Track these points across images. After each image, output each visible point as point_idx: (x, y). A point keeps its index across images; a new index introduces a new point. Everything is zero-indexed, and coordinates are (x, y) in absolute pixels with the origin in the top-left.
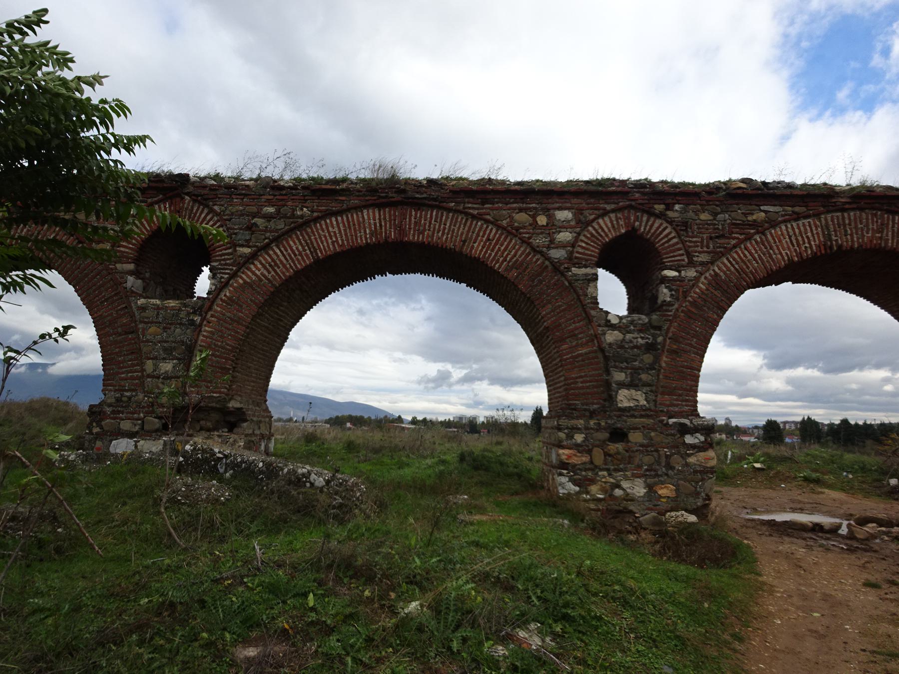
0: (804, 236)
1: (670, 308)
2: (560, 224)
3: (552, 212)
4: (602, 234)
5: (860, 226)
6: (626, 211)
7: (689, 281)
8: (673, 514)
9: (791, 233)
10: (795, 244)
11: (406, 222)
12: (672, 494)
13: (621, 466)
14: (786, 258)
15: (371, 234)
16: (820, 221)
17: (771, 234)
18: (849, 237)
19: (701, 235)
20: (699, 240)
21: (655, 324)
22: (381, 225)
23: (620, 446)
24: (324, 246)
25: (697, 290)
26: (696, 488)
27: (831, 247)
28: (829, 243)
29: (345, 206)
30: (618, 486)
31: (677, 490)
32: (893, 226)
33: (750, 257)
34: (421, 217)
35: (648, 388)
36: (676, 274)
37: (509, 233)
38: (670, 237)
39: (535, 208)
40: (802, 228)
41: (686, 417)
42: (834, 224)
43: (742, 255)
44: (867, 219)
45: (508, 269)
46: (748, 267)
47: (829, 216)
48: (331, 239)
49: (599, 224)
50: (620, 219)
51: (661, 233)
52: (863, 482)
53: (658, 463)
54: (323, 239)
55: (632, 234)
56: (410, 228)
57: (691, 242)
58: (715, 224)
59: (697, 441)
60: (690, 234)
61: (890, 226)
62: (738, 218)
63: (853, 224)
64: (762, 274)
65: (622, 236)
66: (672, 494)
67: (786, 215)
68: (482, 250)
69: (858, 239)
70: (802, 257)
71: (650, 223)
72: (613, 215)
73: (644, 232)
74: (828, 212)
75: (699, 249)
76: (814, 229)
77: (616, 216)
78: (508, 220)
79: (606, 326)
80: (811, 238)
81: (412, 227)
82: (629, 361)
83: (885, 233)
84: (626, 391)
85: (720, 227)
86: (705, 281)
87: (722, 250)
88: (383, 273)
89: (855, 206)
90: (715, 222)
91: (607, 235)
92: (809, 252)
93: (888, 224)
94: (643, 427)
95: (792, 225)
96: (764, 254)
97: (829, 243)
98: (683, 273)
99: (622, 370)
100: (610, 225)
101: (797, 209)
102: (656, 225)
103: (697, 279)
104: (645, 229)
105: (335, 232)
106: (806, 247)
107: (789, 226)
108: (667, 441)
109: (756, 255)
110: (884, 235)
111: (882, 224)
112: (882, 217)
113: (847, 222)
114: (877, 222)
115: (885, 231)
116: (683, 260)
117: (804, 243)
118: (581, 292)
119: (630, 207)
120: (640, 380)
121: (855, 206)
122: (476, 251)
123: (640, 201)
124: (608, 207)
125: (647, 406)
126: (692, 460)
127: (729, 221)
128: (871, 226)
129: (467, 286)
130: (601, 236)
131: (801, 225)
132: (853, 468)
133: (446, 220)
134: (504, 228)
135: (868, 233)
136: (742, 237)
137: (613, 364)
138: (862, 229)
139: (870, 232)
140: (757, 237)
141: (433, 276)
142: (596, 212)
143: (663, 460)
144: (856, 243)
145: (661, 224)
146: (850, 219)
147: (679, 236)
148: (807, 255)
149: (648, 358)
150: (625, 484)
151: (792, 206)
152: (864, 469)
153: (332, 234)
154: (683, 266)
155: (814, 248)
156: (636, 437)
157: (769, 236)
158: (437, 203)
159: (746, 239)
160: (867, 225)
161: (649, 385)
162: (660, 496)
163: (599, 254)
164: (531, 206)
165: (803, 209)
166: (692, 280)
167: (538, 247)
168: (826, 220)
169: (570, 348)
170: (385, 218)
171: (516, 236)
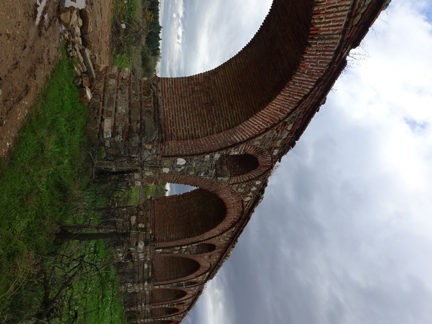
0: (331, 19)
5: (319, 61)
9: (340, 9)
10: (329, 10)
16: (337, 34)
18: (315, 52)
27: (312, 39)
28: (316, 38)
32: (308, 81)
40: (339, 19)
42: (330, 43)
44: (322, 66)
47: (338, 41)
52: (122, 9)
61: (309, 80)
67: (359, 7)
69: (310, 59)
70: (315, 14)
74: (342, 41)
76: (334, 28)
80: (327, 25)
83: (306, 76)
92: (316, 21)
93: (311, 78)
95: (346, 10)
97: (316, 38)
101: (359, 17)
106: (322, 19)
107: (347, 8)
110: (304, 75)
111: (313, 75)
113: (326, 53)
114: (316, 72)
115: (308, 76)
128: (315, 68)
132: (131, 4)
135: (311, 65)
138: (315, 62)
139: (311, 67)
144: (307, 57)
146: (328, 55)
148: (314, 19)
151: (363, 14)
152: (131, 10)
155: (318, 26)
160: (317, 66)
165: (356, 22)
168: (337, 38)
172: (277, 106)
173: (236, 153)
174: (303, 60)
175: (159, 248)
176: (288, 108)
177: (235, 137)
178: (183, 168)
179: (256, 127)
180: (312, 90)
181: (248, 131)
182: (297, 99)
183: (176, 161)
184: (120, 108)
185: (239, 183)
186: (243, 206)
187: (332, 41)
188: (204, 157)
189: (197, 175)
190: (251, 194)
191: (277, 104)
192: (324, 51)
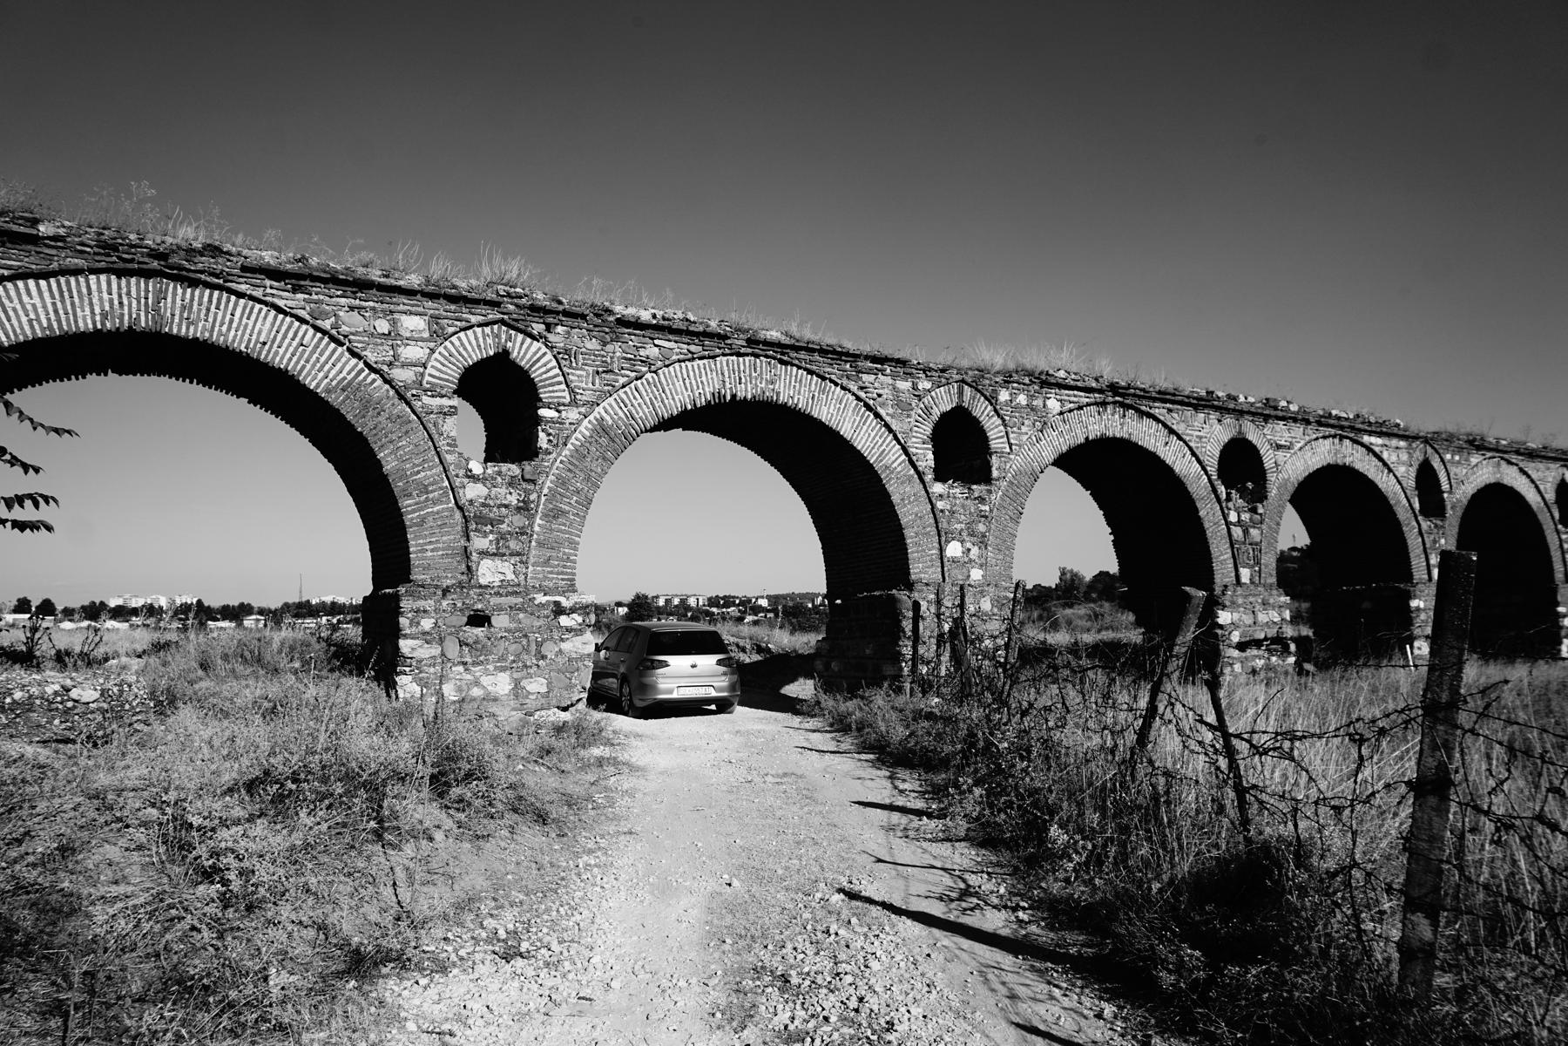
1: (549, 457)
2: (408, 335)
3: (396, 316)
4: (464, 353)
6: (496, 327)
7: (570, 424)
8: (543, 713)
9: (685, 376)
11: (165, 304)
12: (544, 689)
13: (482, 658)
14: (679, 405)
15: (104, 316)
17: (664, 374)
18: (743, 385)
19: (586, 368)
20: (584, 373)
21: (527, 477)
22: (121, 303)
23: (479, 632)
24: (12, 326)
25: (580, 437)
26: (570, 679)
27: (724, 396)
29: (55, 266)
30: (477, 683)
31: (549, 684)
33: (640, 400)
34: (192, 300)
35: (518, 559)
36: (556, 414)
37: (333, 339)
38: (549, 366)
39: (373, 309)
41: (563, 594)
42: (729, 370)
43: (632, 397)
44: (761, 367)
45: (328, 391)
46: (638, 414)
48: (27, 315)
49: (459, 339)
50: (488, 335)
51: (538, 360)
53: (526, 650)
54: (11, 313)
55: (503, 355)
56: (173, 315)
57: (573, 374)
58: (603, 356)
59: (574, 623)
60: (574, 365)
62: (628, 350)
63: (747, 371)
64: (651, 422)
65: (489, 359)
66: (544, 689)
68: (290, 359)
71: (525, 346)
72: (479, 330)
73: (517, 357)
75: (583, 385)
76: (709, 373)
77: (483, 331)
78: (333, 319)
79: (469, 477)
80: (706, 383)
81: (177, 312)
82: (494, 523)
84: (490, 562)
85: (609, 360)
86: (590, 426)
87: (610, 388)
88: (101, 370)
89: (749, 351)
90: (602, 353)
91: (470, 356)
94: (510, 607)
96: (656, 398)
98: (564, 414)
99: (485, 535)
100: (474, 342)
101: (693, 348)
102: (533, 349)
103: (579, 423)
104: (519, 353)
105: (34, 306)
108: (538, 624)
109: (647, 399)
112: (775, 367)
113: (742, 368)
116: (564, 398)
117: (698, 388)
118: (433, 431)
119: (503, 322)
120: (508, 547)
121: (749, 351)
122: (282, 358)
123: (515, 316)
124: (474, 319)
125: (516, 580)
126: (565, 646)
127: (618, 354)
129: (249, 402)
130: (463, 357)
131: (696, 367)
133: (234, 309)
134: (324, 332)
136: (633, 374)
137: (474, 526)
139: (764, 382)
140: (649, 376)
141: (191, 382)
142: (458, 323)
143: (533, 647)
145: (539, 349)
147: (560, 368)
149: (519, 520)
150: (485, 680)
151: (689, 344)
153: (29, 307)
154: (564, 405)
156: (500, 621)
157: (662, 376)
158: (221, 281)
159: (637, 379)
161: (518, 554)
162: (529, 693)
163: (460, 380)
164: (367, 304)
166: (573, 424)
167: (376, 363)
169: (417, 504)
170: (129, 293)
171: (342, 344)
172: (831, 411)
173: (931, 456)
174: (755, 397)
175: (1238, 577)
176: (833, 393)
177: (894, 466)
178: (969, 545)
179: (873, 434)
180: (799, 367)
181: (881, 445)
182: (816, 384)
183: (954, 560)
184: (868, 651)
185: (1007, 433)
186: (1080, 408)
187: (726, 368)
188: (942, 511)
189: (986, 517)
190: (1038, 403)
191: (828, 413)
192: (739, 372)
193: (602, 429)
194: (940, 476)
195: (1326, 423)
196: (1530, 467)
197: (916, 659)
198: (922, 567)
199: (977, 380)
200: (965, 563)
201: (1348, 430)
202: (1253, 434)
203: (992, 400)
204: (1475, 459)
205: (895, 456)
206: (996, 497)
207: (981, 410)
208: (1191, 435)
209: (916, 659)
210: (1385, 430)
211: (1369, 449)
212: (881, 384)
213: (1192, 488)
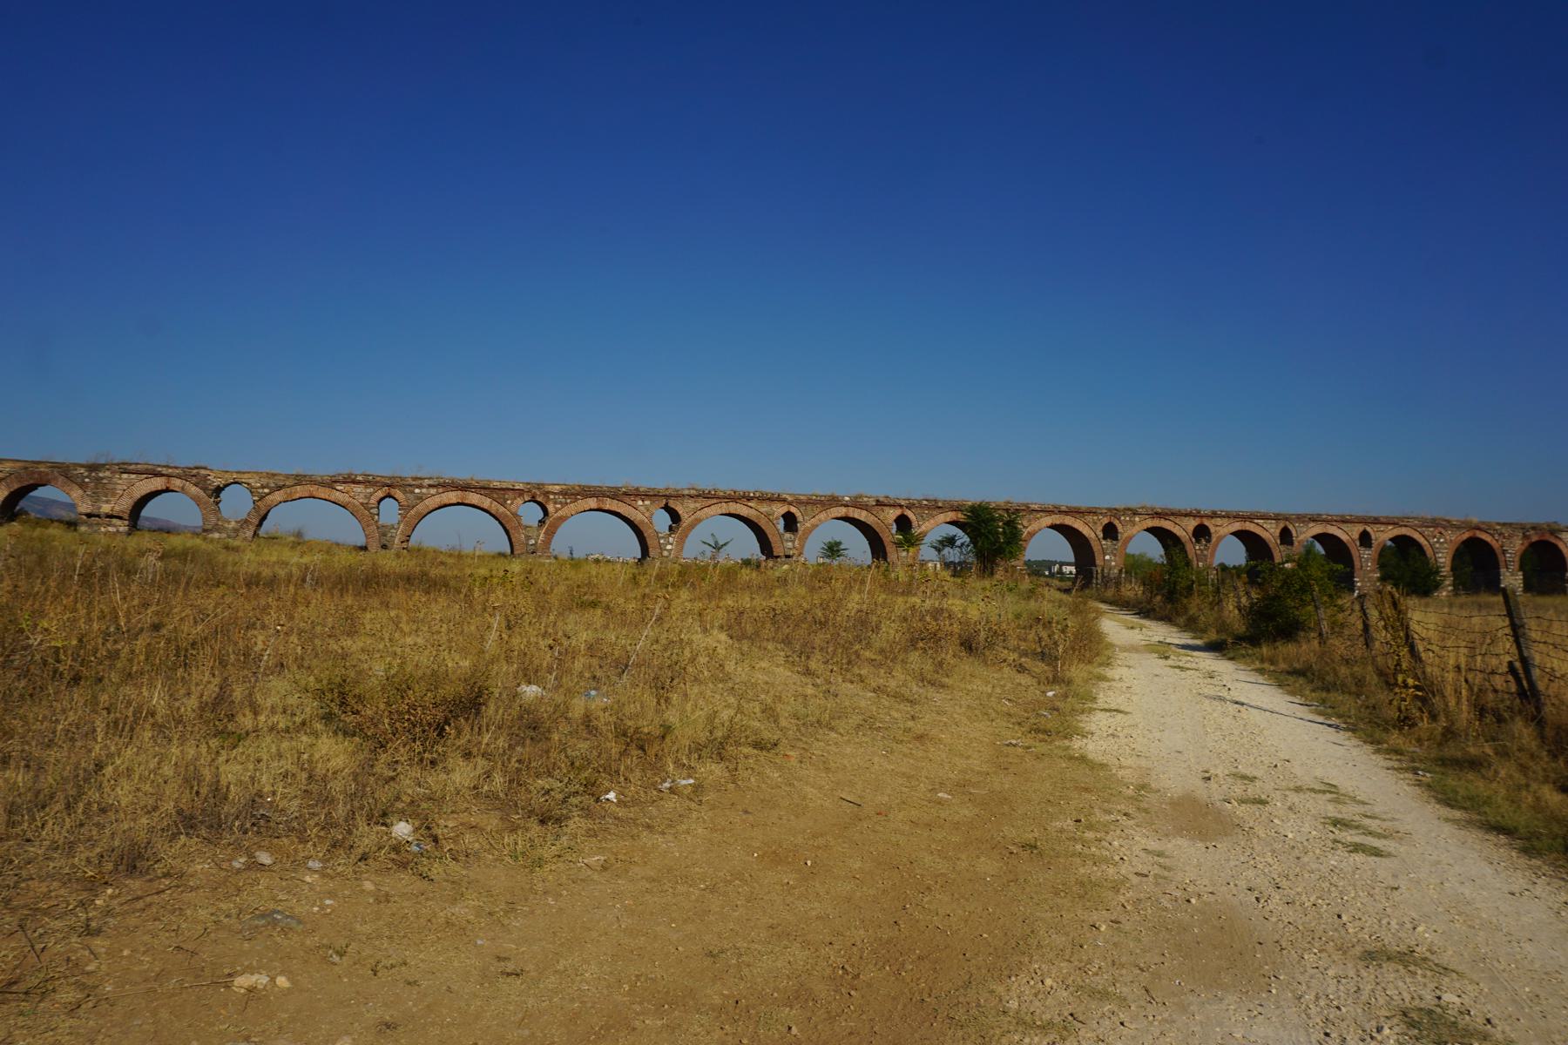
193: (1029, 533)
194: (1104, 538)
195: (1237, 517)
196: (1344, 526)
197: (1097, 584)
198: (1099, 562)
199: (1115, 512)
200: (1110, 561)
201: (1250, 518)
202: (1206, 522)
203: (1119, 519)
204: (1311, 525)
205: (1093, 535)
206: (1119, 544)
207: (1116, 522)
208: (1183, 524)
209: (1097, 584)
210: (1265, 517)
211: (1257, 524)
212: (1089, 518)
213: (1183, 540)
